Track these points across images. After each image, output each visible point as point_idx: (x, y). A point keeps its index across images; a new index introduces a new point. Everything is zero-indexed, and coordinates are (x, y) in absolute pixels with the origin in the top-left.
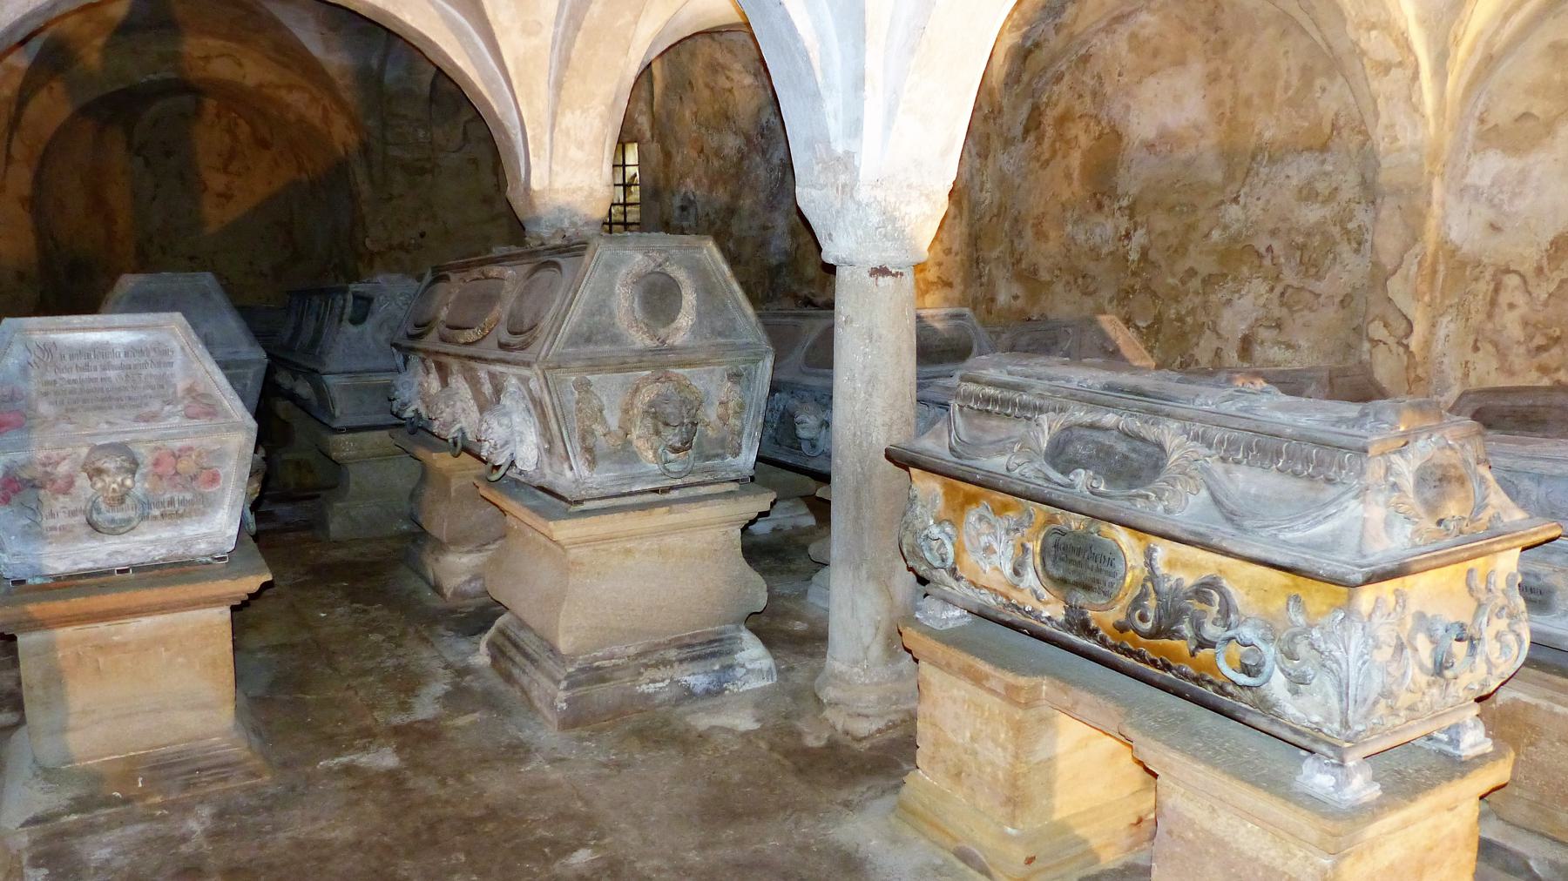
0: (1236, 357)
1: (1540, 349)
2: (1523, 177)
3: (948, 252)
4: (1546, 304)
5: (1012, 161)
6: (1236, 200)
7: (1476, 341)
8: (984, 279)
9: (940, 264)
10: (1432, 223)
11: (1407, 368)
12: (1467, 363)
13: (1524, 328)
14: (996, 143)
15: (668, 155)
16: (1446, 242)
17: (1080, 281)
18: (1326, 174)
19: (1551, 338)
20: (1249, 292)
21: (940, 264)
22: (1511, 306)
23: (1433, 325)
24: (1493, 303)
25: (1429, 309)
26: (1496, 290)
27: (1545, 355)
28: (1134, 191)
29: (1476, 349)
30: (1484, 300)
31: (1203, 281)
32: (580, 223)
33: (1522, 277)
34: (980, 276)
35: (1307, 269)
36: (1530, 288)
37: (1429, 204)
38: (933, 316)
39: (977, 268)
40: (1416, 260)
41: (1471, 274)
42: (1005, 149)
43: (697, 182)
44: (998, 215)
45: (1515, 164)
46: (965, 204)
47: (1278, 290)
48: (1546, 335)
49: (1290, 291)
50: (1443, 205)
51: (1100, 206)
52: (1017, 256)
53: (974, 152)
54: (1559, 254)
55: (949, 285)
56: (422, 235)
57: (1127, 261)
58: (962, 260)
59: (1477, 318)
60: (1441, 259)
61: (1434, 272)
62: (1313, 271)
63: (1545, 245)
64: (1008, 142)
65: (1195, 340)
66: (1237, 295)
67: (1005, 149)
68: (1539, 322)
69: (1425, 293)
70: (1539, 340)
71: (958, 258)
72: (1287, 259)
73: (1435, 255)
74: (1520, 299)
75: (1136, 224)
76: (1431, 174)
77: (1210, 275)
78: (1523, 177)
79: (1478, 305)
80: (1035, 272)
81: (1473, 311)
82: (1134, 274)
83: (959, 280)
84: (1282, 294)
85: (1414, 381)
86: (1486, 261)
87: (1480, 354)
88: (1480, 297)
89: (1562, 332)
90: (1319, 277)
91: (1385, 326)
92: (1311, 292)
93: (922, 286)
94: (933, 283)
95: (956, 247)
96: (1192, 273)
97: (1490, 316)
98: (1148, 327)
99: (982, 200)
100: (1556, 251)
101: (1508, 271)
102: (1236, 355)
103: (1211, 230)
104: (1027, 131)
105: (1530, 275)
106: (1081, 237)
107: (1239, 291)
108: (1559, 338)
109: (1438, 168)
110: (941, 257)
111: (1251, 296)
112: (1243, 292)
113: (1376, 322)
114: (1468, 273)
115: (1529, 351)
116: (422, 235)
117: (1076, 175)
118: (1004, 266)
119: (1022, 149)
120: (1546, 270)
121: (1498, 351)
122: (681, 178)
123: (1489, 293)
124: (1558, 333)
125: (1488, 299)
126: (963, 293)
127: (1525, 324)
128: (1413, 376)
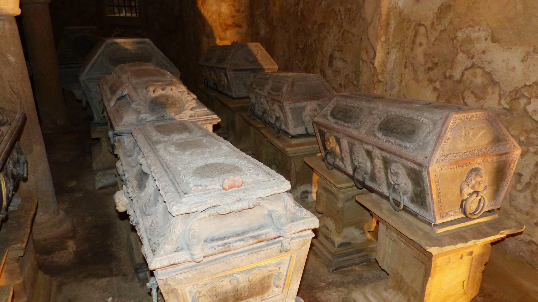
1: (430, 69)
3: (238, 11)
4: (434, 44)
7: (406, 63)
9: (233, 17)
12: (402, 74)
13: (425, 57)
16: (396, 8)
20: (332, 33)
21: (233, 17)
22: (421, 44)
23: (388, 53)
24: (414, 42)
25: (385, 44)
26: (415, 36)
29: (406, 67)
33: (426, 28)
35: (351, 22)
36: (428, 35)
38: (125, 43)
40: (378, 18)
47: (342, 32)
48: (432, 61)
49: (346, 32)
54: (442, 15)
55: (240, 26)
57: (298, 16)
58: (246, 15)
59: (408, 50)
60: (392, 17)
61: (388, 24)
62: (353, 22)
63: (436, 10)
66: (328, 34)
69: (382, 36)
70: (430, 65)
71: (244, 14)
73: (388, 15)
74: (424, 41)
77: (321, 24)
81: (405, 46)
83: (245, 24)
84: (343, 34)
85: (377, 82)
86: (412, 18)
87: (407, 70)
88: (409, 39)
89: (439, 60)
92: (351, 33)
94: (230, 25)
95: (242, 9)
96: (315, 22)
97: (412, 49)
100: (440, 14)
101: (420, 25)
105: (429, 27)
107: (329, 32)
110: (234, 13)
112: (330, 33)
114: (405, 26)
115: (425, 70)
121: (413, 69)
124: (437, 61)
125: (412, 40)
127: (425, 55)
128: (376, 80)
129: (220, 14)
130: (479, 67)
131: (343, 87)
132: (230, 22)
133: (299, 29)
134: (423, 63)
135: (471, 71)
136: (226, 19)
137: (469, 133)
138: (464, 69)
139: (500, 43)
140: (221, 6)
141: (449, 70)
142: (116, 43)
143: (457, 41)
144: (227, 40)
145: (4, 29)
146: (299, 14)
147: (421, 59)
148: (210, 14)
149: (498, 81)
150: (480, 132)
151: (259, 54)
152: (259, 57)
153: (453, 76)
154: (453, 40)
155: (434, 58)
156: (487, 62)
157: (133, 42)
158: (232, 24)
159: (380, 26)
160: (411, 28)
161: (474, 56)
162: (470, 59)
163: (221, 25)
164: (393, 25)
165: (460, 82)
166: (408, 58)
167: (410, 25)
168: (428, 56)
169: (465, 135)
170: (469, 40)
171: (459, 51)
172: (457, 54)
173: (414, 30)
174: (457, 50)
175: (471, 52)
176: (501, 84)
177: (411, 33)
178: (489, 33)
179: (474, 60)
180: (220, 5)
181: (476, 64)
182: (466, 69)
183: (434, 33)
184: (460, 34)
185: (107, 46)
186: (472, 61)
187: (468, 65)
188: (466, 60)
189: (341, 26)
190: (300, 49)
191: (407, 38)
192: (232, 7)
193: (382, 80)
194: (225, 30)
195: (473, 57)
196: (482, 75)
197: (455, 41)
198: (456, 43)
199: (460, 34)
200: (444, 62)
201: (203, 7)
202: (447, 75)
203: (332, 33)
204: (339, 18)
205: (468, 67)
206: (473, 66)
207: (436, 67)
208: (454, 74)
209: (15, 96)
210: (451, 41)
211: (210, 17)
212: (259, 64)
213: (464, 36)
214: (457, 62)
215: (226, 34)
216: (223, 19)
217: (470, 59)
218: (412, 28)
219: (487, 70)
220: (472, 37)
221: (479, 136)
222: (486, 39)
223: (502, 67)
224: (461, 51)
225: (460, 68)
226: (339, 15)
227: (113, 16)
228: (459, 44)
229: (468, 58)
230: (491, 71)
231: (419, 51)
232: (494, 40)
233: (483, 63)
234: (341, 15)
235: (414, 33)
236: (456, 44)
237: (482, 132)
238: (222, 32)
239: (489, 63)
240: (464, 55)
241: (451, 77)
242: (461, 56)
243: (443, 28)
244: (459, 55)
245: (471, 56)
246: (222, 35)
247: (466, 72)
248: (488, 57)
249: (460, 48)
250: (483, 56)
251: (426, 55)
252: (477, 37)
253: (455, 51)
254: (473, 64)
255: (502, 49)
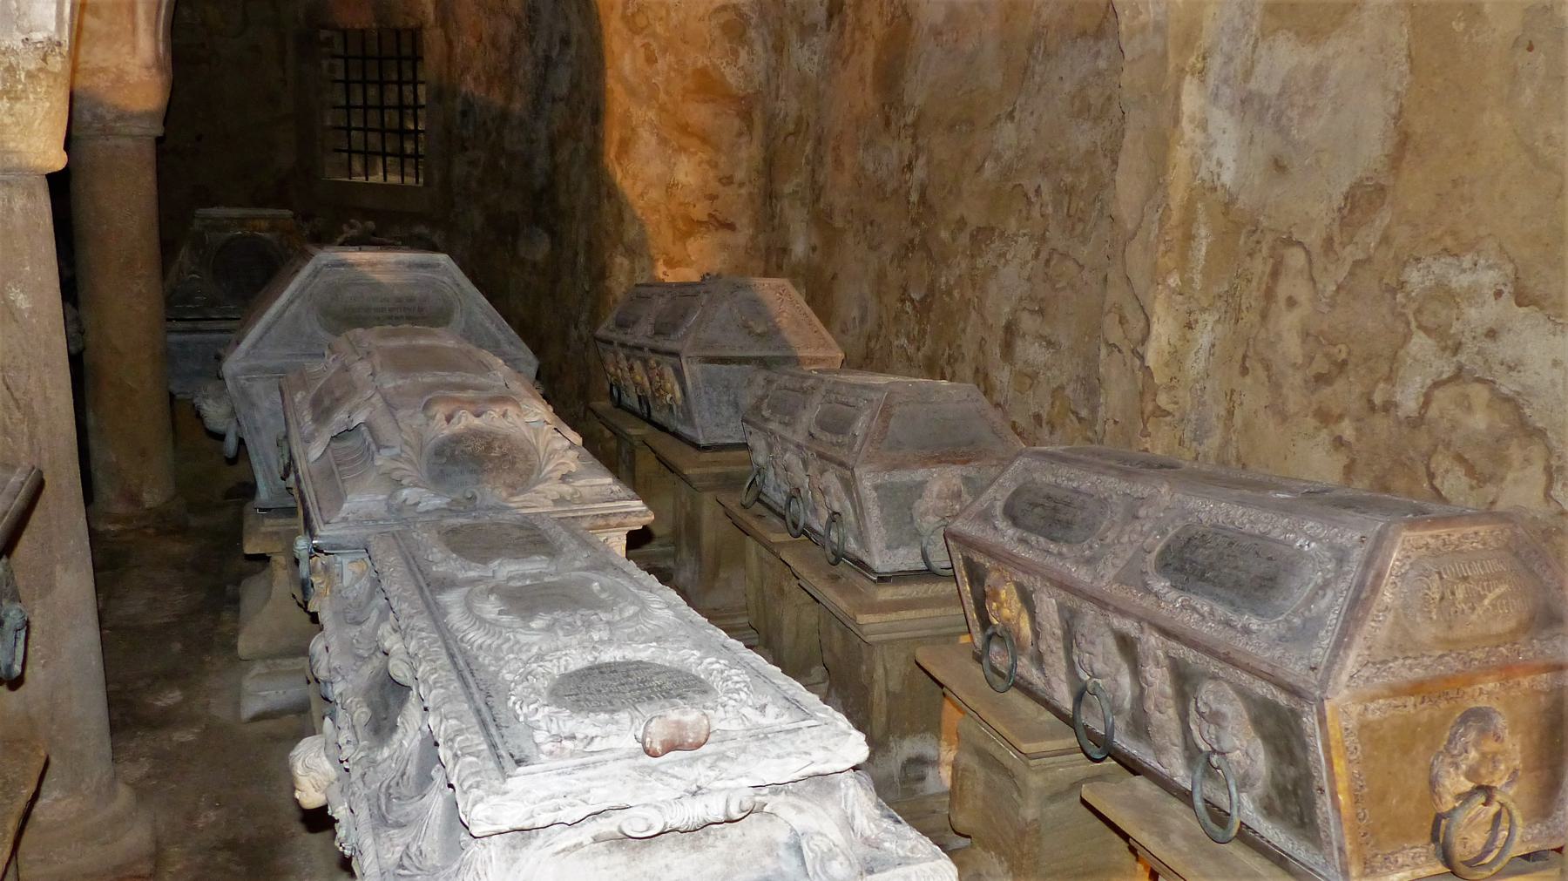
0: (999, 355)
1: (1321, 379)
2: (1320, 73)
3: (727, 181)
5: (816, 59)
6: (1011, 116)
7: (1245, 357)
8: (776, 221)
10: (1181, 155)
11: (1142, 394)
12: (1232, 392)
13: (1304, 342)
14: (792, 34)
15: (450, 43)
16: (1215, 189)
17: (869, 227)
18: (1099, 74)
19: (1335, 363)
22: (1292, 302)
23: (1189, 326)
24: (1269, 295)
25: (1180, 298)
26: (1275, 274)
27: (1327, 391)
28: (919, 101)
29: (1244, 371)
30: (1259, 289)
31: (972, 236)
32: (109, 116)
33: (1308, 253)
34: (773, 217)
35: (1073, 225)
36: (1316, 275)
37: (1176, 121)
38: (372, 264)
39: (771, 205)
40: (1157, 216)
41: (1245, 243)
42: (803, 41)
43: (476, 79)
44: (795, 133)
45: (1311, 57)
46: (757, 116)
47: (1044, 255)
48: (1327, 355)
49: (1056, 257)
50: (1203, 125)
51: (887, 123)
52: (817, 192)
53: (769, 44)
54: (1358, 214)
55: (730, 227)
56: (199, 138)
57: (908, 202)
58: (750, 194)
59: (1251, 318)
60: (1202, 217)
61: (1189, 237)
62: (1079, 227)
63: (1338, 201)
64: (806, 31)
65: (961, 325)
67: (803, 41)
68: (1322, 332)
69: (1169, 272)
70: (1320, 366)
72: (1055, 207)
73: (1189, 208)
74: (1303, 293)
75: (918, 148)
76: (1181, 72)
77: (979, 229)
78: (1320, 73)
79: (1251, 297)
80: (830, 215)
81: (1244, 307)
82: (915, 223)
84: (1048, 262)
85: (1153, 414)
86: (1265, 222)
87: (1248, 380)
88: (1254, 283)
89: (1349, 353)
90: (1084, 239)
91: (1120, 322)
93: (681, 224)
94: (700, 223)
95: (740, 175)
96: (962, 223)
97: (1264, 316)
98: (922, 300)
99: (777, 111)
100: (1351, 211)
101: (1290, 242)
102: (998, 351)
103: (984, 162)
104: (830, 16)
105: (1316, 249)
106: (870, 167)
107: (1004, 255)
108: (1345, 363)
109: (1193, 59)
111: (1017, 261)
112: (1009, 257)
113: (1112, 314)
114: (1241, 242)
116: (199, 138)
117: (869, 79)
118: (803, 205)
119: (821, 41)
120: (1336, 246)
121: (1269, 377)
122: (462, 74)
123: (1265, 278)
124: (1343, 356)
125: (1264, 286)
126: (753, 238)
127: (1306, 335)
128: (1150, 407)
129: (670, 187)
130: (1479, 380)
131: (1044, 425)
132: (700, 211)
133: (911, 241)
134: (1300, 361)
135: (1452, 390)
136: (689, 203)
137: (1453, 593)
138: (1429, 382)
139: (1542, 308)
140: (675, 164)
141: (1382, 385)
142: (342, 264)
143: (1408, 295)
144: (687, 266)
145: (10, 210)
146: (914, 197)
147: (1292, 346)
148: (639, 187)
149: (1539, 425)
150: (1490, 592)
151: (785, 314)
152: (784, 321)
153: (1396, 405)
154: (1394, 292)
155: (1335, 345)
156: (1502, 364)
157: (398, 263)
158: (705, 218)
159: (1165, 242)
160: (1260, 251)
161: (1460, 344)
162: (1448, 353)
163: (673, 220)
164: (1204, 242)
165: (1417, 422)
166: (1251, 342)
167: (1258, 242)
168: (1317, 338)
169: (1442, 598)
170: (1444, 294)
171: (1413, 325)
172: (1407, 337)
173: (1271, 257)
174: (1408, 324)
175: (1452, 331)
176: (1549, 434)
177: (1260, 267)
178: (1507, 275)
179: (1463, 358)
180: (673, 160)
181: (1468, 371)
182: (1437, 385)
183: (1332, 268)
184: (1414, 276)
185: (316, 273)
186: (1455, 359)
187: (1442, 372)
188: (1435, 355)
189: (1043, 239)
190: (912, 301)
191: (1249, 281)
192: (708, 167)
193: (1170, 408)
194: (684, 236)
195: (1457, 348)
196: (1488, 406)
197: (1400, 297)
198: (1404, 301)
199: (1414, 276)
200: (1366, 360)
201: (620, 164)
202: (1378, 399)
203: (1015, 256)
204: (1036, 213)
205: (1445, 376)
206: (1459, 375)
207: (1340, 372)
208: (1398, 398)
209: (18, 415)
210: (1388, 296)
211: (642, 195)
212: (786, 345)
213: (1427, 283)
214: (1409, 361)
215: (686, 249)
216: (681, 204)
217: (1448, 353)
218: (1265, 251)
219: (1504, 390)
220: (1454, 285)
221: (1486, 602)
222: (1498, 294)
223: (1554, 384)
224: (1420, 327)
225: (1418, 379)
226: (1037, 207)
227: (347, 180)
228: (1414, 306)
229: (1444, 349)
230: (1519, 394)
231: (1288, 323)
232: (1522, 299)
233: (1490, 369)
234: (1042, 205)
235: (1268, 269)
236: (1404, 306)
237: (1498, 591)
238: (674, 244)
239: (1510, 368)
240: (1430, 341)
241: (1389, 406)
242: (1420, 343)
243: (1361, 256)
244: (1413, 341)
245: (1450, 343)
246: (675, 251)
247: (1438, 393)
248: (1505, 349)
249: (1416, 320)
250: (1488, 345)
251: (1308, 334)
252: (1470, 288)
253: (1401, 328)
254: (1460, 368)
255: (1550, 325)
